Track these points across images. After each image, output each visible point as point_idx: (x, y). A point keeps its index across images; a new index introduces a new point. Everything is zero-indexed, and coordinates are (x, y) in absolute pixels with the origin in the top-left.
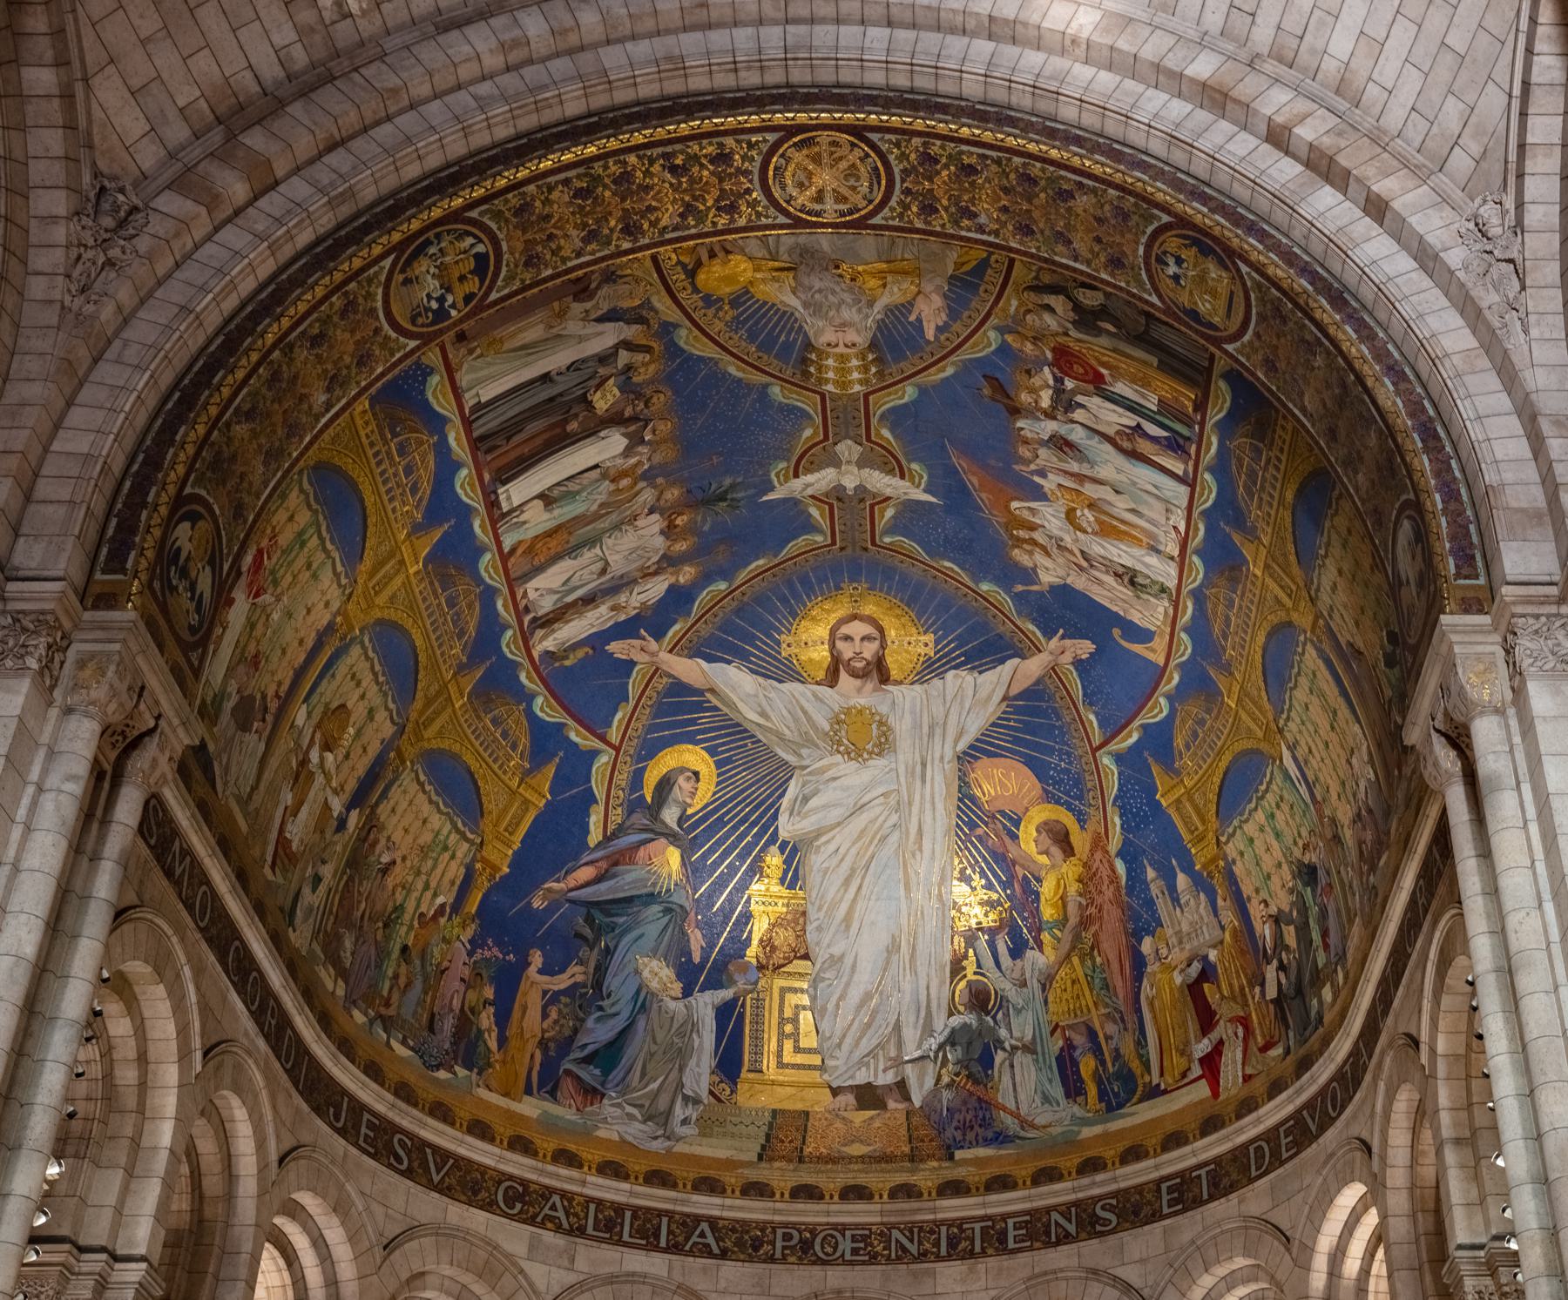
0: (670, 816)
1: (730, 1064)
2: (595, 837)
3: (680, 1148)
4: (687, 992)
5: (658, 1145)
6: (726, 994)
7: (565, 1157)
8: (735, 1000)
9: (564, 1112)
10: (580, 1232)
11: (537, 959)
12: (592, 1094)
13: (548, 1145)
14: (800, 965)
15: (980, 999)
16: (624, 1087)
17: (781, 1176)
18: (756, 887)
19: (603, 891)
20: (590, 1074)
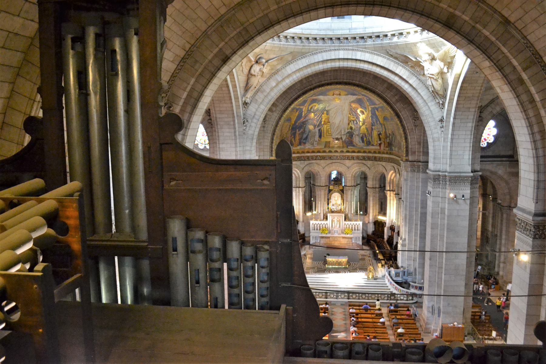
0: (312, 110)
1: (320, 136)
2: (303, 114)
3: (315, 147)
4: (315, 128)
5: (313, 148)
6: (319, 128)
7: (303, 152)
8: (320, 129)
9: (302, 147)
10: (305, 160)
11: (297, 130)
12: (305, 143)
13: (300, 151)
14: (329, 123)
15: (351, 128)
16: (308, 141)
17: (327, 150)
18: (323, 115)
19: (305, 120)
20: (304, 141)
